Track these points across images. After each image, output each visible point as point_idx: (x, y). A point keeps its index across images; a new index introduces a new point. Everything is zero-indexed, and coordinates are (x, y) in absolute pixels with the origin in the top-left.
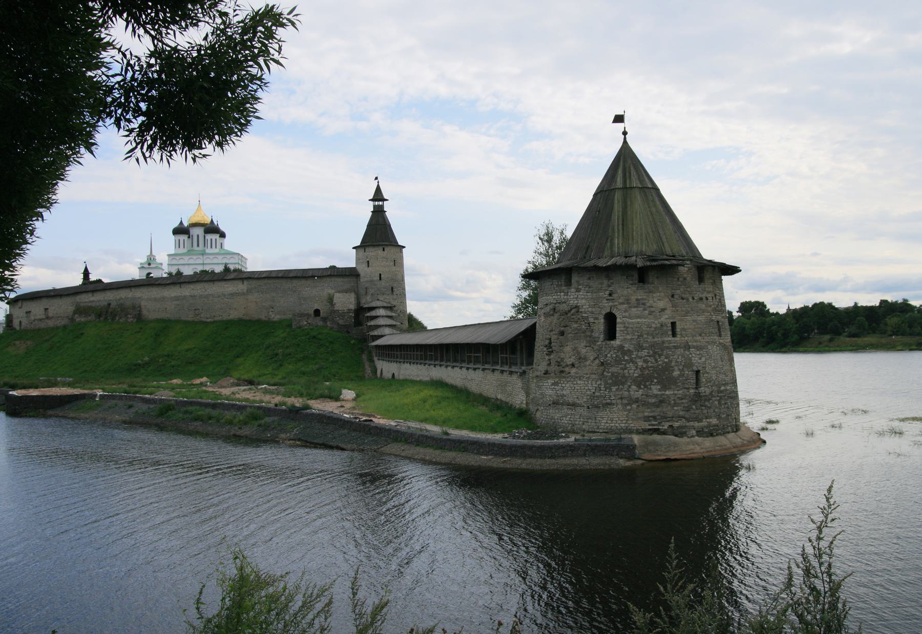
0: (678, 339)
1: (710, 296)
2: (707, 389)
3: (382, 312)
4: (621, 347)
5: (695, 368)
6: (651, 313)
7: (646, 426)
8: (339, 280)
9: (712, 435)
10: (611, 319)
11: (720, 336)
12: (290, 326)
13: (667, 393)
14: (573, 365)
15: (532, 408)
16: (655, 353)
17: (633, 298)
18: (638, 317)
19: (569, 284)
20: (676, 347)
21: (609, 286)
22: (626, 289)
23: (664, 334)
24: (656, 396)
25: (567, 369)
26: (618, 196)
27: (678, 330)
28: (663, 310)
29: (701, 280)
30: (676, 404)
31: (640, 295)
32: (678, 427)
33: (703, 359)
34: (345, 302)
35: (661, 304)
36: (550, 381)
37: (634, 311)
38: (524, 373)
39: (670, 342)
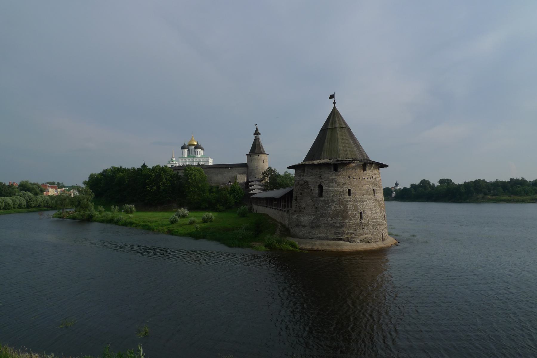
2: (366, 221)
3: (257, 183)
4: (324, 201)
5: (360, 211)
6: (338, 185)
7: (335, 237)
8: (239, 169)
9: (368, 242)
10: (321, 187)
11: (375, 196)
12: (218, 188)
13: (345, 222)
14: (304, 208)
15: (290, 227)
16: (340, 203)
17: (331, 178)
19: (304, 172)
21: (320, 173)
22: (328, 174)
24: (339, 223)
25: (302, 210)
26: (329, 132)
27: (351, 193)
28: (344, 184)
29: (364, 170)
30: (350, 227)
31: (334, 177)
32: (351, 238)
34: (242, 178)
36: (296, 215)
38: (288, 211)
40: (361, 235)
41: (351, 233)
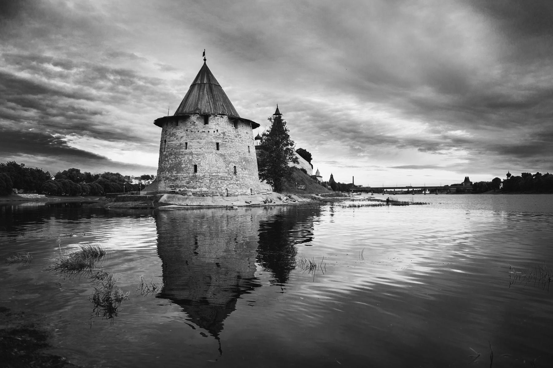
0: (188, 151)
1: (211, 131)
5: (194, 164)
7: (169, 190)
9: (203, 196)
11: (218, 149)
18: (173, 141)
20: (185, 154)
23: (181, 148)
28: (182, 137)
29: (206, 122)
30: (183, 180)
33: (200, 160)
35: (181, 135)
37: (172, 138)
39: (183, 152)
40: (193, 188)
41: (184, 186)
